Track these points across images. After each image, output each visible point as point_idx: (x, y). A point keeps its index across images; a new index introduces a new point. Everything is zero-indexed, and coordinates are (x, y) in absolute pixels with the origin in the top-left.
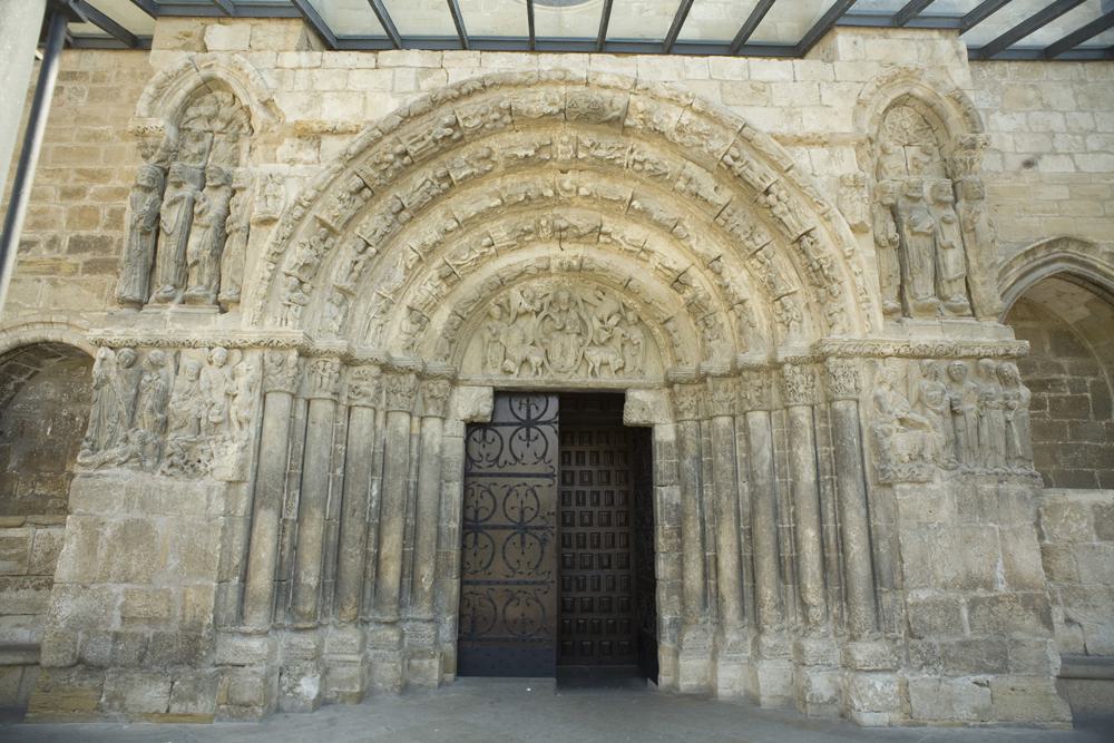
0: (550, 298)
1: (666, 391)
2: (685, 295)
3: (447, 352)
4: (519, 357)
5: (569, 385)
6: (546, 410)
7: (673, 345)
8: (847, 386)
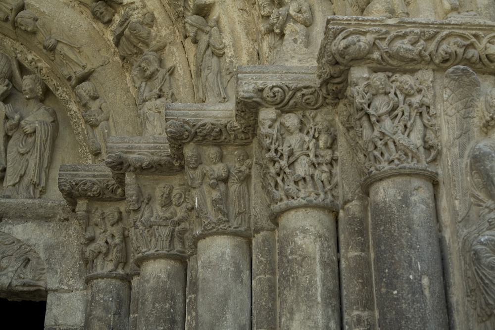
8: (401, 138)
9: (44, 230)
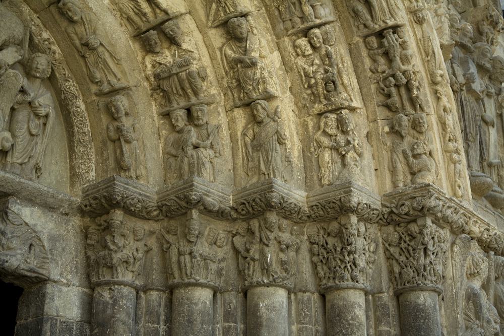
9: (48, 219)
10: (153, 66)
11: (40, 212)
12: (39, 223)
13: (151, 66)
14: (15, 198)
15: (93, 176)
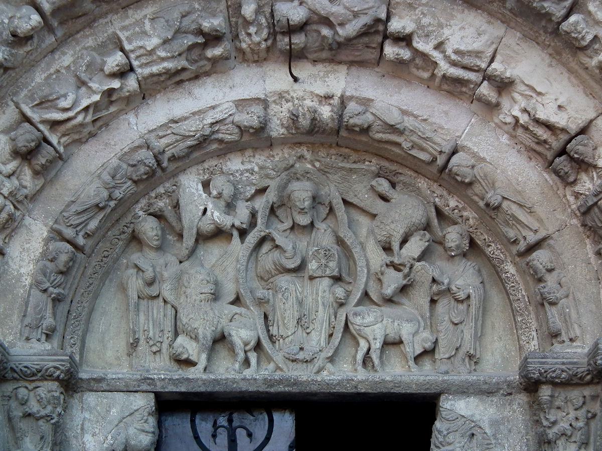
0: (271, 196)
1: (522, 398)
2: (577, 188)
3: (49, 321)
4: (206, 332)
5: (314, 388)
6: (267, 439)
7: (543, 302)
10: (577, 198)
11: (477, 401)
12: (477, 412)
13: (574, 197)
14: (447, 395)
15: (534, 346)
